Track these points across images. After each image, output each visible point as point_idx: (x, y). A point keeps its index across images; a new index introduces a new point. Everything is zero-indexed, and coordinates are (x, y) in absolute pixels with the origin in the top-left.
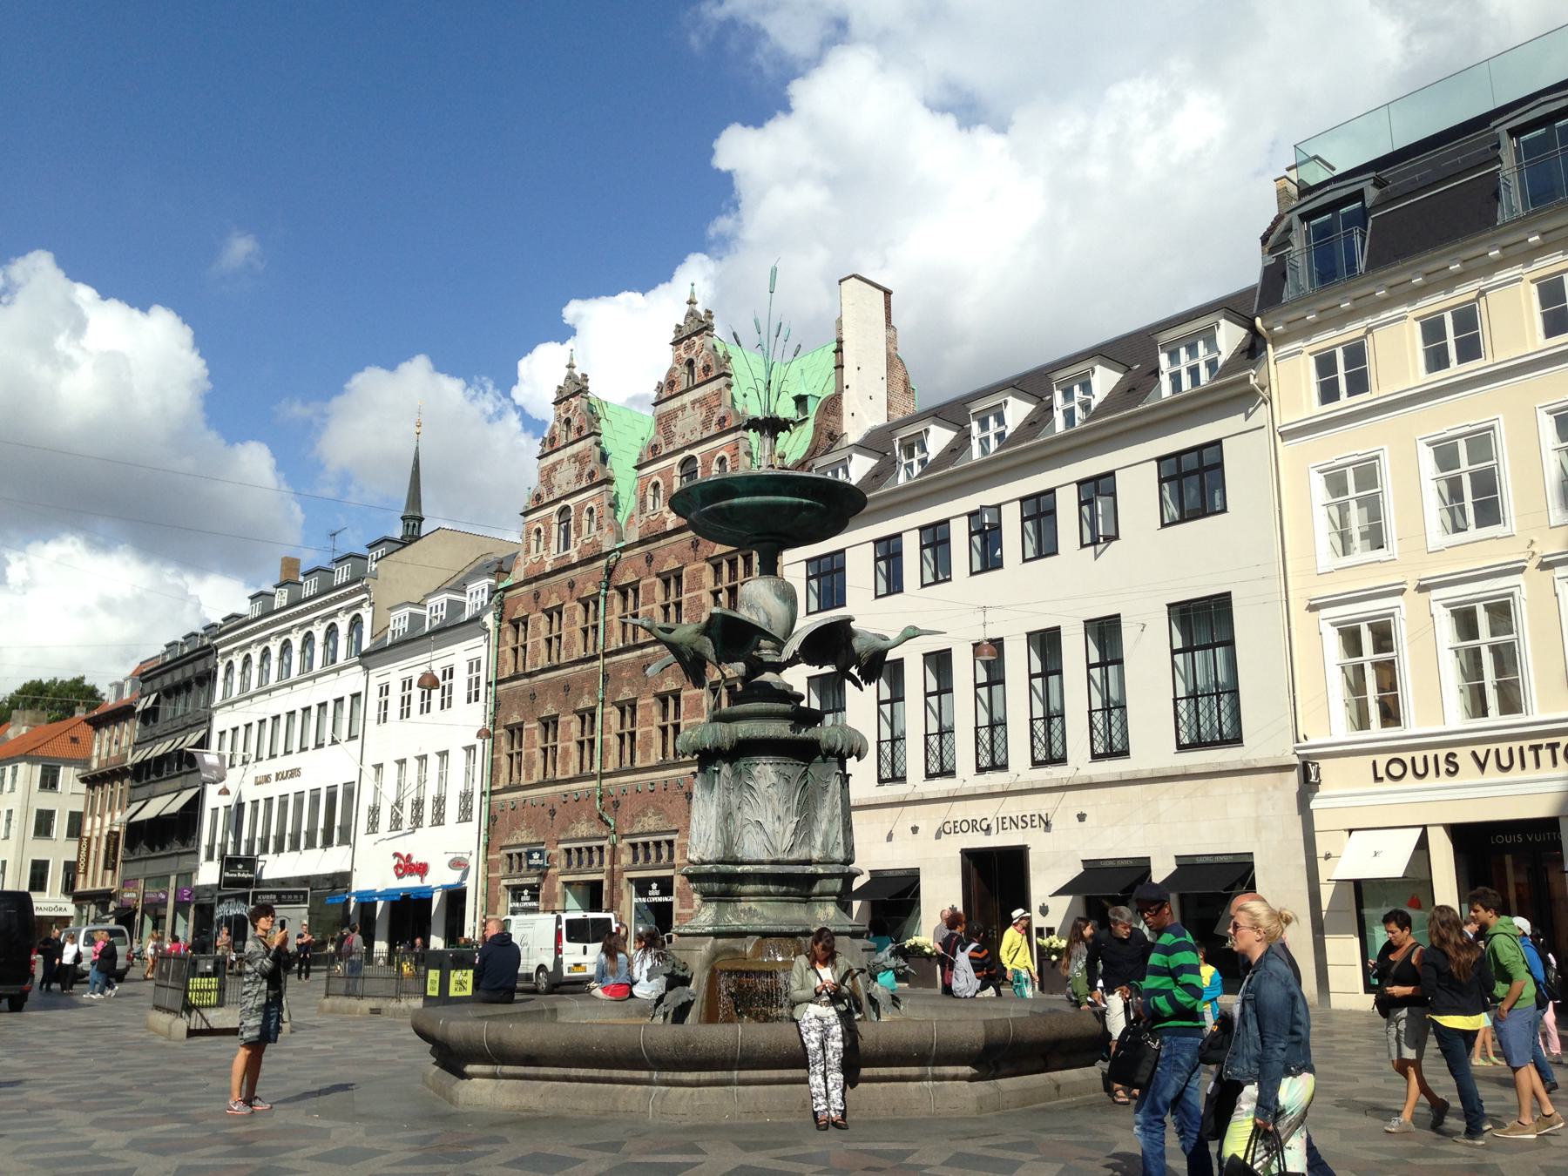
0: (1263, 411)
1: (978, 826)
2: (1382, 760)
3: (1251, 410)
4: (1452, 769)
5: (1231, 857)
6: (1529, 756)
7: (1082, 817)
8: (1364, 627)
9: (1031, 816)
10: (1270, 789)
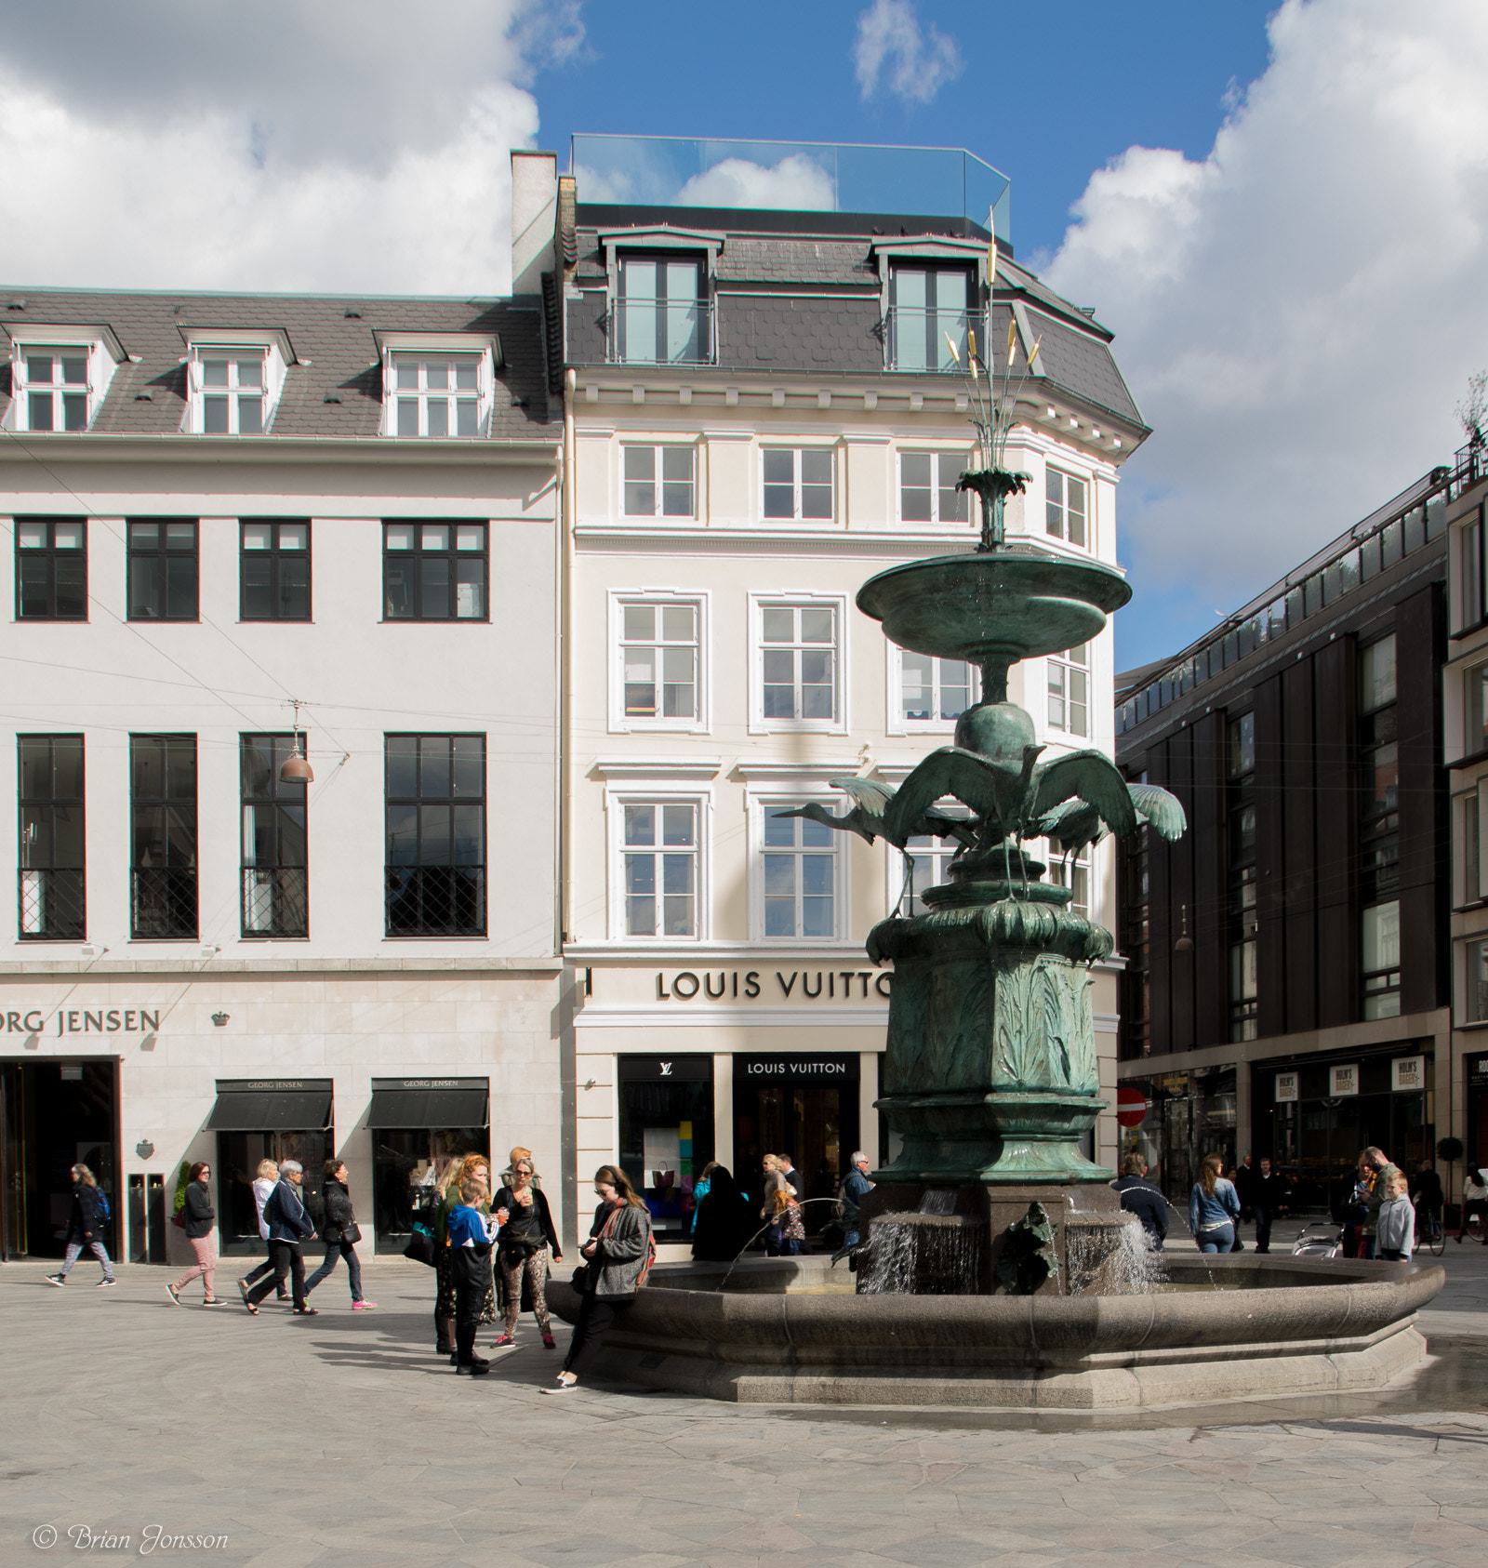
0: (552, 500)
1: (21, 1023)
2: (670, 975)
3: (533, 495)
4: (752, 991)
5: (455, 1083)
6: (839, 984)
7: (220, 1020)
8: (659, 810)
9: (128, 1013)
10: (520, 998)
